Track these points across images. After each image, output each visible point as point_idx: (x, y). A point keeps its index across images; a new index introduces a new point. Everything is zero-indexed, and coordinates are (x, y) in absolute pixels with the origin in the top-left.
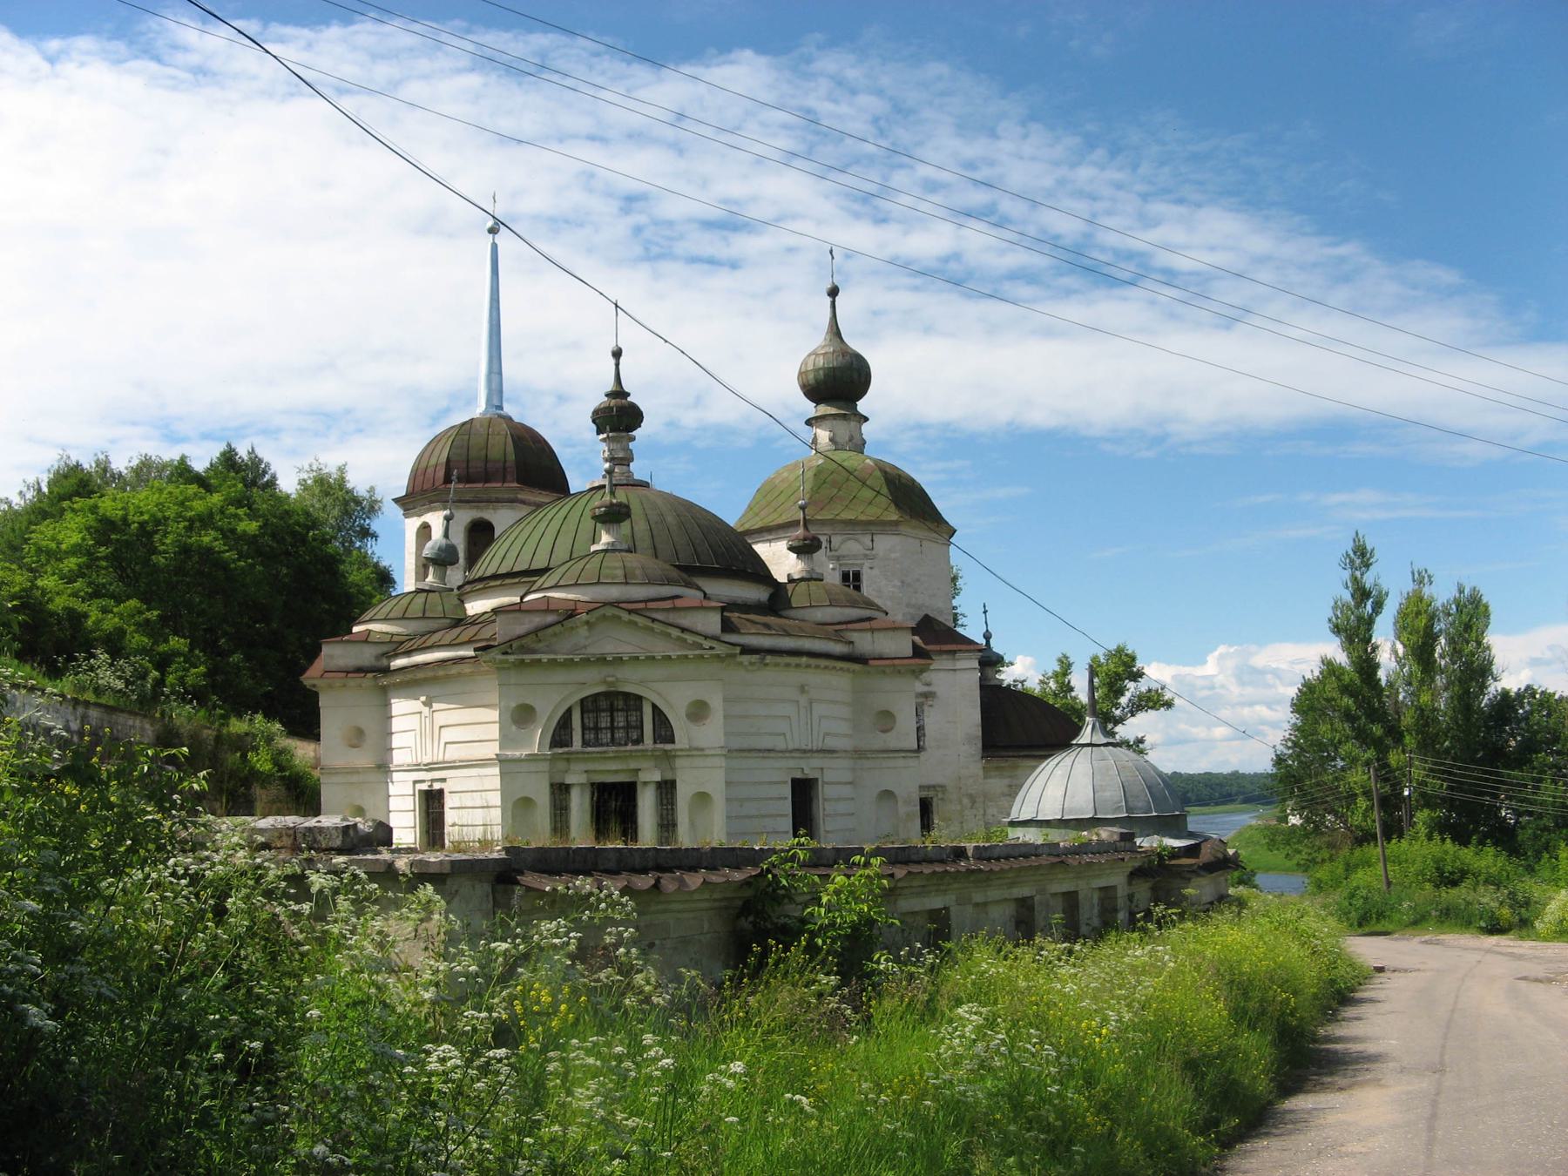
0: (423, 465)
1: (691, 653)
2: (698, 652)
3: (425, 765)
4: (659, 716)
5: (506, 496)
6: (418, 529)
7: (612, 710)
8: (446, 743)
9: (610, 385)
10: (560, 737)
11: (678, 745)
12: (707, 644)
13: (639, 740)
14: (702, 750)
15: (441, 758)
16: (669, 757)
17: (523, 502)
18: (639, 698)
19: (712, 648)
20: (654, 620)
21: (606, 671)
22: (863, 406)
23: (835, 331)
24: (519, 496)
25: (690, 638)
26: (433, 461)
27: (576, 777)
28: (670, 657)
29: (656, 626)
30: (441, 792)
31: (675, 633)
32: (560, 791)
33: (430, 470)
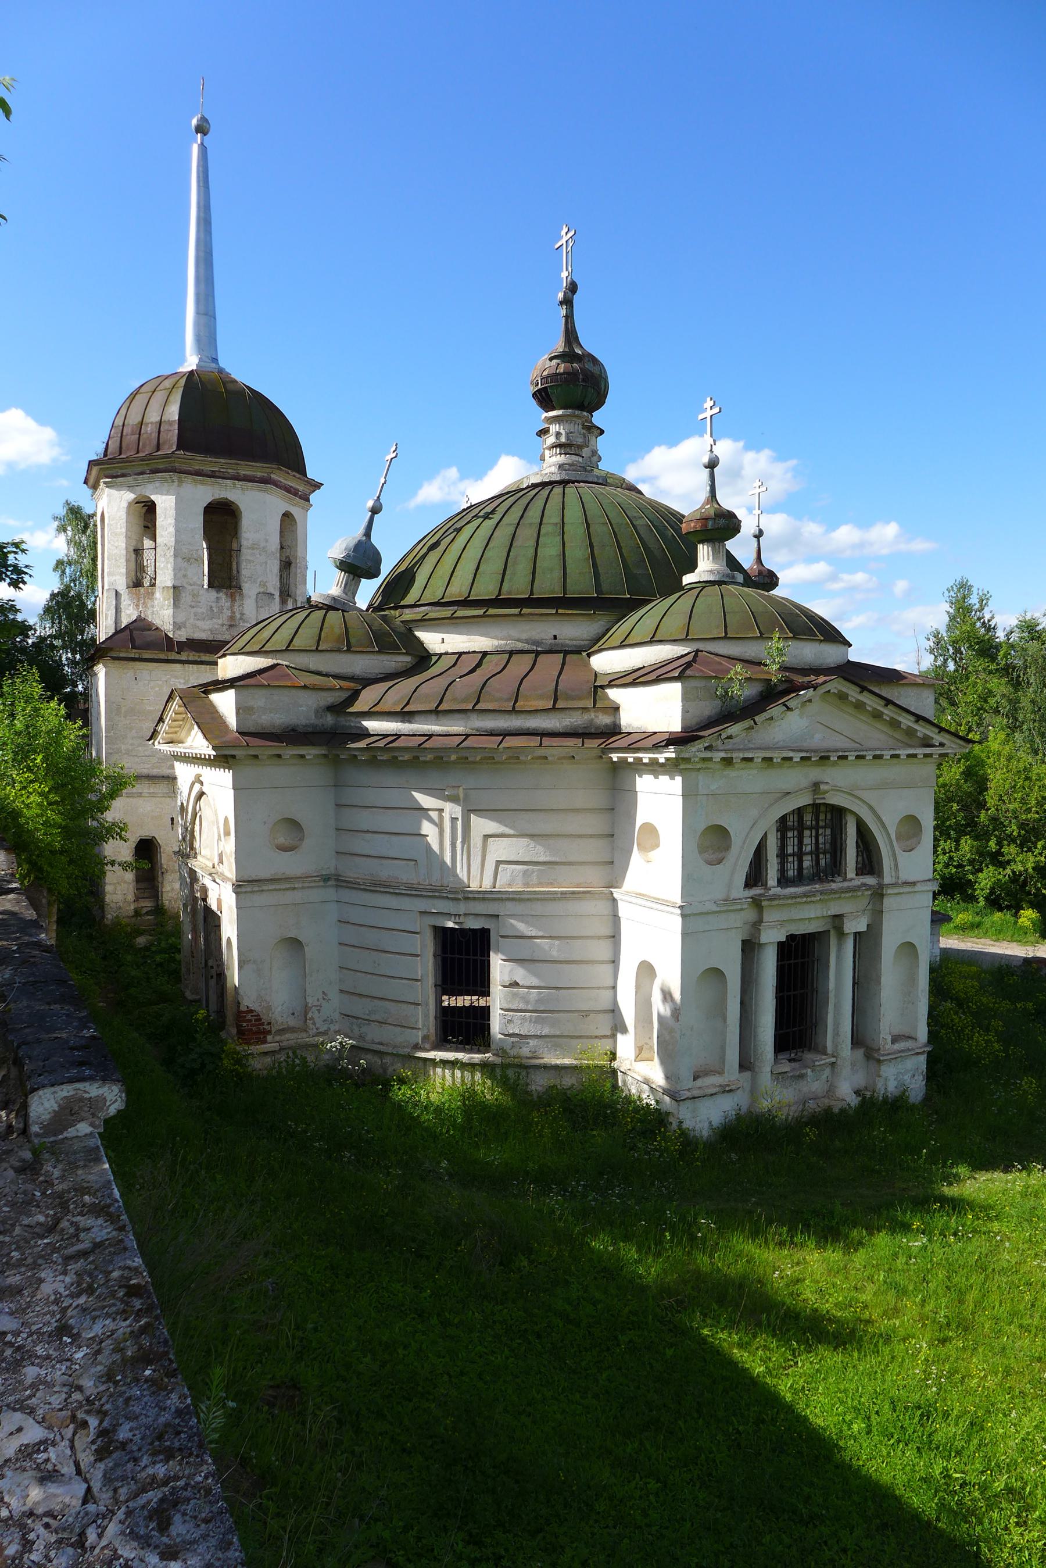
0: (134, 419)
1: (920, 751)
2: (928, 750)
3: (451, 892)
4: (864, 836)
5: (259, 474)
6: (130, 504)
7: (801, 827)
8: (499, 863)
9: (559, 345)
10: (755, 877)
11: (887, 879)
12: (938, 738)
13: (835, 868)
14: (913, 884)
15: (487, 885)
16: (878, 894)
17: (276, 484)
18: (838, 813)
19: (942, 745)
20: (888, 702)
21: (815, 773)
22: (598, 418)
23: (571, 335)
24: (272, 476)
25: (922, 730)
26: (153, 417)
27: (772, 936)
28: (897, 756)
29: (888, 712)
30: (485, 933)
31: (907, 721)
32: (750, 948)
33: (149, 429)
